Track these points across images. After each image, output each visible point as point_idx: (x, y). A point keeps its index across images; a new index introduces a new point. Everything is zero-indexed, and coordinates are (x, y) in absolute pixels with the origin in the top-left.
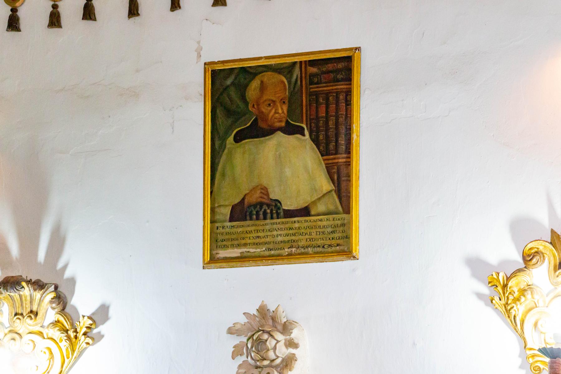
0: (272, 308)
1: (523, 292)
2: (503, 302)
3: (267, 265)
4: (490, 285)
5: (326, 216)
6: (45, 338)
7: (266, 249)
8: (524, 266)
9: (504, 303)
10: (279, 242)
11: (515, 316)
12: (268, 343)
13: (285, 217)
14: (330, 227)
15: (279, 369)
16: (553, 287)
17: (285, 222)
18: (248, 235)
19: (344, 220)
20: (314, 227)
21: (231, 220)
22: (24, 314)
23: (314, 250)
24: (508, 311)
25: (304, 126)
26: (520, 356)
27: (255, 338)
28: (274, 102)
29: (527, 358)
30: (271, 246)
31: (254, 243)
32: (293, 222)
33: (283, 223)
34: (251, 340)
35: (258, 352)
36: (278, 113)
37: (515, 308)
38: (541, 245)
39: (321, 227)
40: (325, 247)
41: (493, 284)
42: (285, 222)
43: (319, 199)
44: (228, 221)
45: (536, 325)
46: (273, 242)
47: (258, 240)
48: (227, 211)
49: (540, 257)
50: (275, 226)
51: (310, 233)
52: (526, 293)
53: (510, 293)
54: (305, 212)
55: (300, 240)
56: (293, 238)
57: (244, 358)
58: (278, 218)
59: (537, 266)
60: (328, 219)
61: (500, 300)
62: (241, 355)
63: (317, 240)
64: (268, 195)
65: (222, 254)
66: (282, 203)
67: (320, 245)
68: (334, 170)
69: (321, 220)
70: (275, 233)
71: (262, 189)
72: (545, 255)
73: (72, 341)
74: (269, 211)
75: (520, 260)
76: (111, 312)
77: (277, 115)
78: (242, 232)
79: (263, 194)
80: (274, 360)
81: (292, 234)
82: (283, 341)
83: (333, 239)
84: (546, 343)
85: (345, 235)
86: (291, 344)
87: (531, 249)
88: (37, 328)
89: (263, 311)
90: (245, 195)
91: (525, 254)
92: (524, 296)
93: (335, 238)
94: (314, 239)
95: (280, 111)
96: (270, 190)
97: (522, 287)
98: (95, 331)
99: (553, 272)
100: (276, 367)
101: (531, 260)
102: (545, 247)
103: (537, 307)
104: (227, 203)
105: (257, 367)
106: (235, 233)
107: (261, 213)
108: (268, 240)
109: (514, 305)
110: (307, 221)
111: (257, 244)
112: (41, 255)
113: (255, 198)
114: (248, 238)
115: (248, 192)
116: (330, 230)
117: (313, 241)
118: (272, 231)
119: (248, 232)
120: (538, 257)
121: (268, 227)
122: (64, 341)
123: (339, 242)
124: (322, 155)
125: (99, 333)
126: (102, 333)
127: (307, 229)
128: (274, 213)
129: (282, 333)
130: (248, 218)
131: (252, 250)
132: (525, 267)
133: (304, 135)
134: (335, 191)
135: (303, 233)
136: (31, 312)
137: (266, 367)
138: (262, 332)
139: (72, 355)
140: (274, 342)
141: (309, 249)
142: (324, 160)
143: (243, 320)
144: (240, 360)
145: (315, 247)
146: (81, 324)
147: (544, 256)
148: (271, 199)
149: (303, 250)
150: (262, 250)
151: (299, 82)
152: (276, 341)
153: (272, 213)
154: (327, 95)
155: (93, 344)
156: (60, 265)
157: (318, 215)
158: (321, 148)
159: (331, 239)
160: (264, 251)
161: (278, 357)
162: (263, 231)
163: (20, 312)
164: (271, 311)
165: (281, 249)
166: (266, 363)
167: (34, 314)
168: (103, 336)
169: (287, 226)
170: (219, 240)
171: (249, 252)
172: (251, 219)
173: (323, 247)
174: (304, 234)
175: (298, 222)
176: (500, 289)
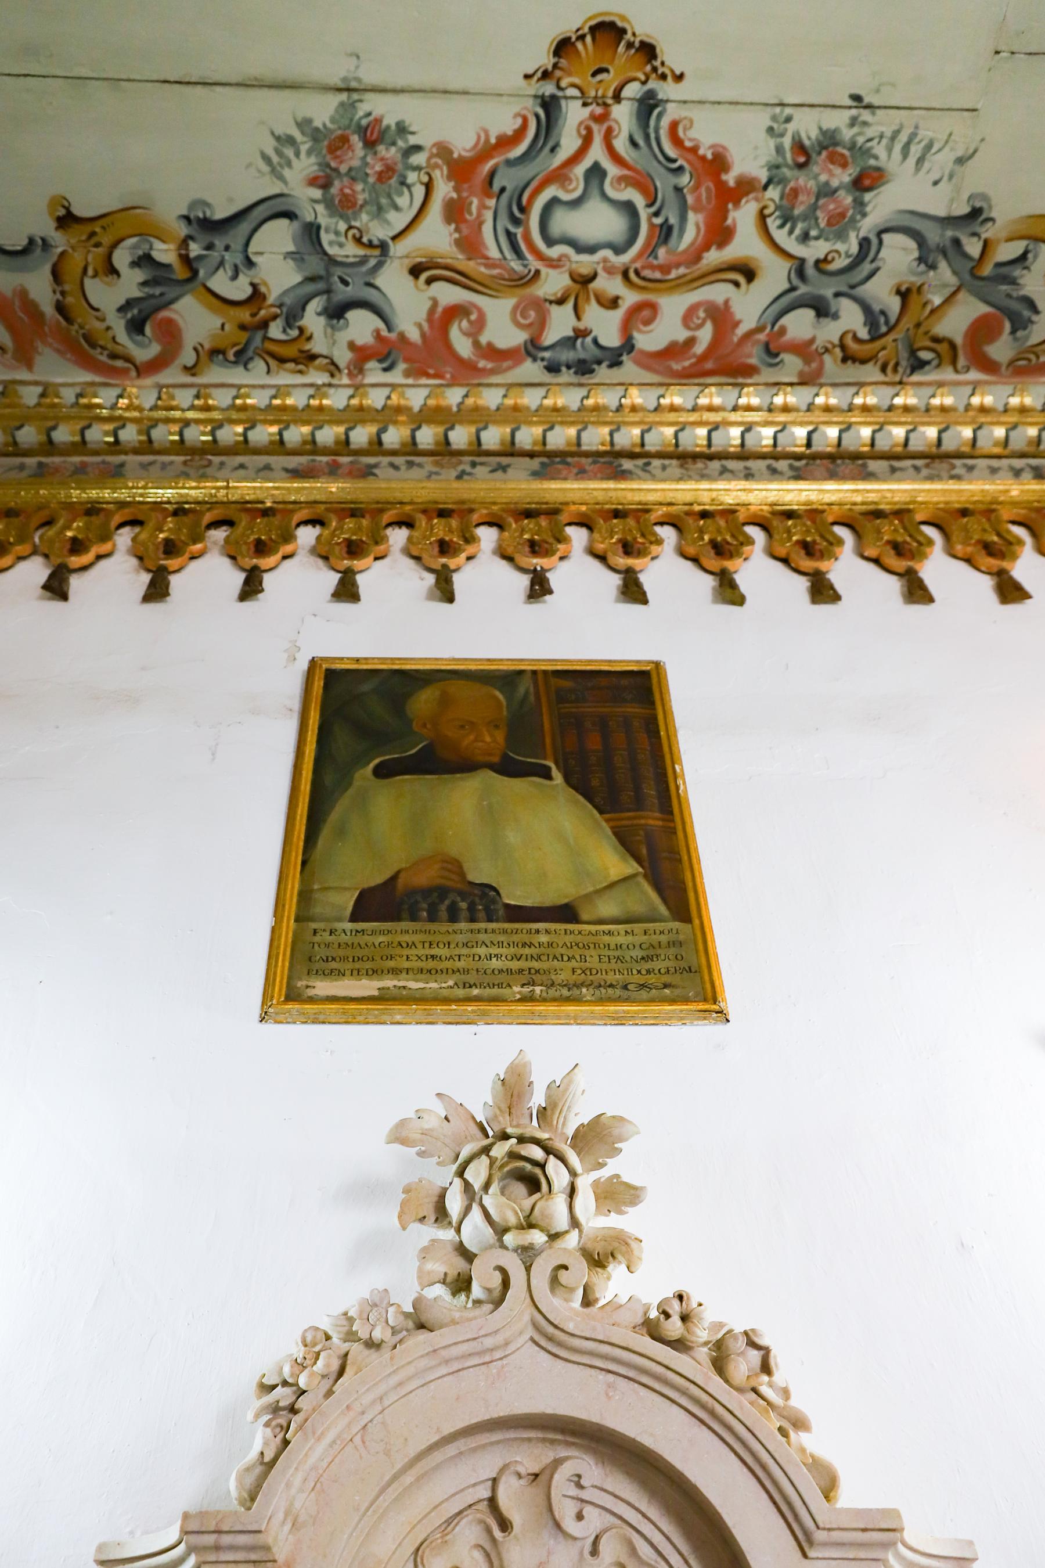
3: (457, 1023)
7: (456, 984)
10: (493, 971)
13: (510, 920)
14: (637, 947)
17: (509, 931)
18: (406, 952)
19: (677, 933)
20: (592, 946)
21: (354, 918)
23: (597, 992)
28: (472, 724)
30: (471, 978)
31: (422, 969)
32: (533, 931)
33: (505, 932)
36: (483, 741)
39: (612, 946)
42: (509, 931)
43: (598, 892)
44: (348, 918)
46: (477, 970)
47: (431, 964)
50: (482, 937)
51: (583, 957)
55: (556, 970)
56: (536, 965)
58: (490, 920)
60: (629, 931)
63: (604, 973)
64: (462, 874)
65: (323, 987)
66: (501, 891)
67: (614, 983)
68: (638, 838)
69: (610, 933)
70: (482, 951)
71: (446, 862)
74: (464, 905)
77: (480, 744)
78: (386, 943)
79: (449, 871)
81: (532, 956)
83: (648, 972)
85: (684, 964)
90: (398, 872)
93: (656, 971)
94: (594, 971)
95: (488, 739)
96: (466, 866)
104: (346, 884)
106: (366, 945)
107: (443, 907)
108: (461, 964)
111: (430, 971)
113: (424, 878)
114: (405, 958)
115: (408, 866)
116: (638, 953)
117: (591, 974)
118: (473, 947)
119: (404, 945)
121: (460, 938)
123: (666, 979)
124: (601, 812)
127: (572, 947)
128: (479, 910)
130: (405, 915)
131: (413, 985)
134: (645, 876)
135: (562, 955)
142: (607, 821)
145: (600, 986)
148: (470, 883)
149: (565, 992)
150: (444, 985)
151: (532, 698)
153: (472, 908)
154: (603, 724)
157: (601, 922)
158: (597, 800)
159: (644, 972)
162: (447, 946)
165: (500, 986)
169: (516, 938)
170: (318, 957)
171: (404, 987)
172: (414, 918)
173: (625, 987)
174: (565, 958)
175: (547, 932)
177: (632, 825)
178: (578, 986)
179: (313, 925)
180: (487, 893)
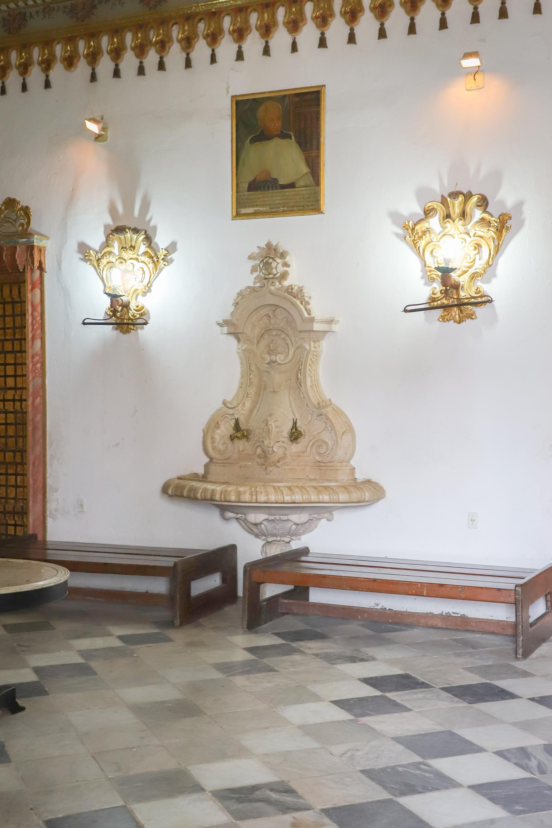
0: (274, 243)
1: (424, 233)
2: (412, 238)
4: (404, 229)
5: (304, 188)
6: (139, 262)
8: (424, 217)
9: (412, 239)
11: (419, 247)
12: (272, 264)
15: (278, 280)
16: (442, 229)
22: (127, 248)
25: (292, 134)
26: (422, 271)
27: (264, 261)
29: (426, 272)
34: (262, 263)
35: (266, 270)
37: (419, 242)
38: (435, 204)
40: (305, 206)
41: (405, 228)
43: (300, 178)
45: (432, 252)
48: (246, 186)
49: (435, 212)
52: (426, 234)
53: (416, 234)
54: (292, 186)
57: (258, 273)
58: (276, 189)
59: (432, 217)
61: (410, 237)
62: (256, 271)
65: (243, 211)
69: (302, 190)
70: (274, 198)
72: (438, 210)
73: (156, 264)
74: (270, 185)
75: (422, 213)
76: (178, 246)
80: (275, 275)
82: (281, 264)
83: (309, 202)
84: (438, 263)
86: (286, 265)
87: (429, 207)
88: (135, 256)
89: (269, 245)
91: (425, 210)
92: (425, 235)
97: (423, 230)
98: (169, 257)
99: (442, 221)
100: (277, 278)
101: (429, 213)
102: (437, 205)
103: (432, 242)
105: (265, 279)
107: (266, 186)
109: (418, 240)
110: (294, 191)
111: (264, 205)
112: (136, 213)
116: (307, 196)
120: (433, 212)
122: (151, 263)
124: (302, 152)
125: (171, 258)
126: (173, 258)
129: (280, 258)
131: (261, 209)
132: (425, 218)
133: (291, 139)
134: (311, 173)
136: (131, 246)
137: (271, 278)
138: (268, 258)
139: (156, 272)
140: (276, 264)
141: (295, 208)
142: (304, 154)
143: (257, 251)
144: (255, 274)
146: (161, 253)
147: (437, 211)
148: (272, 178)
149: (291, 209)
152: (277, 263)
155: (167, 265)
156: (147, 219)
160: (268, 209)
161: (278, 273)
163: (125, 247)
164: (274, 245)
166: (271, 276)
167: (133, 247)
168: (173, 260)
171: (259, 210)
172: (260, 190)
173: (303, 207)
175: (288, 191)
176: (410, 231)
177: (310, 156)
178: (294, 207)
179: (240, 194)
180: (276, 180)
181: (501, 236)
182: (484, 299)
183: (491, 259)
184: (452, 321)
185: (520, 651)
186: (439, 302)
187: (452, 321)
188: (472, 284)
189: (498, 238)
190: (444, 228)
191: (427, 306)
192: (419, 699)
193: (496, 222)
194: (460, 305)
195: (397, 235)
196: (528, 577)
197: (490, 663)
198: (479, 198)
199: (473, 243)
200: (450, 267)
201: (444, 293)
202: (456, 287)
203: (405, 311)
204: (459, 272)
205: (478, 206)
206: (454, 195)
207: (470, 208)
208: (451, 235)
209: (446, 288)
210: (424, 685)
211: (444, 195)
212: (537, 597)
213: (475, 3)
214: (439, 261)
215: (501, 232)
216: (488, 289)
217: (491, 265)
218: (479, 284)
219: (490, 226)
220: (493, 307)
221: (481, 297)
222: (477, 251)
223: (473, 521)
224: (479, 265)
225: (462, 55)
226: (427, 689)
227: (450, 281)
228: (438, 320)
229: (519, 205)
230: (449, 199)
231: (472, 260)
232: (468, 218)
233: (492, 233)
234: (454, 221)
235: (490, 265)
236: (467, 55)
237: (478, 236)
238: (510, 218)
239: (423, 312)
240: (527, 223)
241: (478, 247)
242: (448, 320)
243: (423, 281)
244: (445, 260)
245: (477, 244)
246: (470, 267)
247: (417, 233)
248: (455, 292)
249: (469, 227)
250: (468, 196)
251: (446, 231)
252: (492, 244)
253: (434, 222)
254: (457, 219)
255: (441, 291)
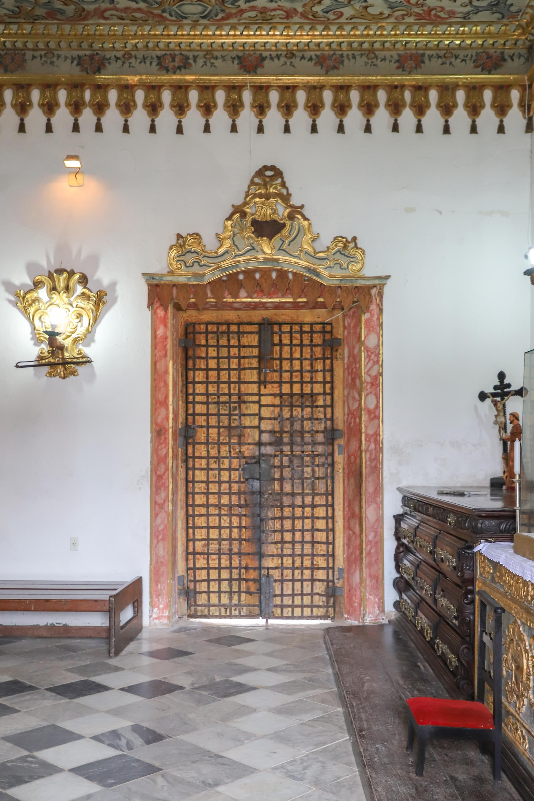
1: (34, 301)
16: (48, 299)
24: (26, 311)
26: (32, 333)
29: (36, 334)
41: (17, 295)
45: (40, 318)
75: (32, 284)
84: (46, 328)
99: (49, 292)
102: (45, 279)
176: (21, 299)
181: (99, 308)
182: (84, 360)
183: (90, 327)
184: (58, 377)
185: (113, 651)
186: (47, 360)
187: (58, 377)
188: (75, 347)
189: (96, 310)
190: (51, 298)
191: (36, 363)
192: (27, 700)
193: (95, 297)
194: (65, 363)
195: (10, 301)
196: (120, 589)
197: (88, 663)
198: (80, 276)
199: (75, 313)
200: (56, 331)
201: (51, 353)
202: (62, 348)
203: (17, 366)
204: (64, 336)
205: (79, 282)
206: (60, 271)
207: (73, 284)
208: (57, 305)
209: (53, 349)
210: (31, 688)
211: (51, 270)
212: (127, 605)
213: (76, 116)
214: (47, 326)
215: (99, 305)
216: (89, 351)
217: (91, 332)
218: (80, 347)
219: (89, 300)
220: (92, 366)
221: (82, 357)
222: (78, 320)
223: (74, 544)
224: (81, 331)
225: (65, 157)
226: (33, 691)
227: (56, 343)
228: (46, 375)
229: (113, 285)
230: (55, 275)
231: (74, 326)
232: (72, 291)
233: (90, 306)
234: (59, 293)
235: (90, 332)
236: (70, 157)
237: (80, 308)
238: (106, 294)
239: (32, 368)
240: (119, 300)
241: (79, 316)
242: (54, 376)
243: (33, 342)
244: (52, 325)
245: (79, 314)
246: (73, 333)
247: (28, 301)
248: (60, 352)
249: (72, 299)
250: (71, 273)
251: (53, 301)
252: (91, 315)
253: (42, 293)
254: (62, 292)
255: (48, 352)
